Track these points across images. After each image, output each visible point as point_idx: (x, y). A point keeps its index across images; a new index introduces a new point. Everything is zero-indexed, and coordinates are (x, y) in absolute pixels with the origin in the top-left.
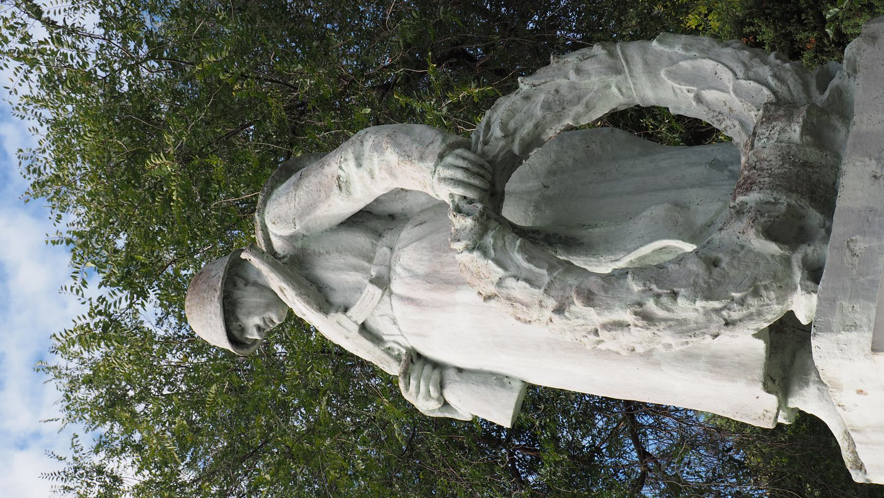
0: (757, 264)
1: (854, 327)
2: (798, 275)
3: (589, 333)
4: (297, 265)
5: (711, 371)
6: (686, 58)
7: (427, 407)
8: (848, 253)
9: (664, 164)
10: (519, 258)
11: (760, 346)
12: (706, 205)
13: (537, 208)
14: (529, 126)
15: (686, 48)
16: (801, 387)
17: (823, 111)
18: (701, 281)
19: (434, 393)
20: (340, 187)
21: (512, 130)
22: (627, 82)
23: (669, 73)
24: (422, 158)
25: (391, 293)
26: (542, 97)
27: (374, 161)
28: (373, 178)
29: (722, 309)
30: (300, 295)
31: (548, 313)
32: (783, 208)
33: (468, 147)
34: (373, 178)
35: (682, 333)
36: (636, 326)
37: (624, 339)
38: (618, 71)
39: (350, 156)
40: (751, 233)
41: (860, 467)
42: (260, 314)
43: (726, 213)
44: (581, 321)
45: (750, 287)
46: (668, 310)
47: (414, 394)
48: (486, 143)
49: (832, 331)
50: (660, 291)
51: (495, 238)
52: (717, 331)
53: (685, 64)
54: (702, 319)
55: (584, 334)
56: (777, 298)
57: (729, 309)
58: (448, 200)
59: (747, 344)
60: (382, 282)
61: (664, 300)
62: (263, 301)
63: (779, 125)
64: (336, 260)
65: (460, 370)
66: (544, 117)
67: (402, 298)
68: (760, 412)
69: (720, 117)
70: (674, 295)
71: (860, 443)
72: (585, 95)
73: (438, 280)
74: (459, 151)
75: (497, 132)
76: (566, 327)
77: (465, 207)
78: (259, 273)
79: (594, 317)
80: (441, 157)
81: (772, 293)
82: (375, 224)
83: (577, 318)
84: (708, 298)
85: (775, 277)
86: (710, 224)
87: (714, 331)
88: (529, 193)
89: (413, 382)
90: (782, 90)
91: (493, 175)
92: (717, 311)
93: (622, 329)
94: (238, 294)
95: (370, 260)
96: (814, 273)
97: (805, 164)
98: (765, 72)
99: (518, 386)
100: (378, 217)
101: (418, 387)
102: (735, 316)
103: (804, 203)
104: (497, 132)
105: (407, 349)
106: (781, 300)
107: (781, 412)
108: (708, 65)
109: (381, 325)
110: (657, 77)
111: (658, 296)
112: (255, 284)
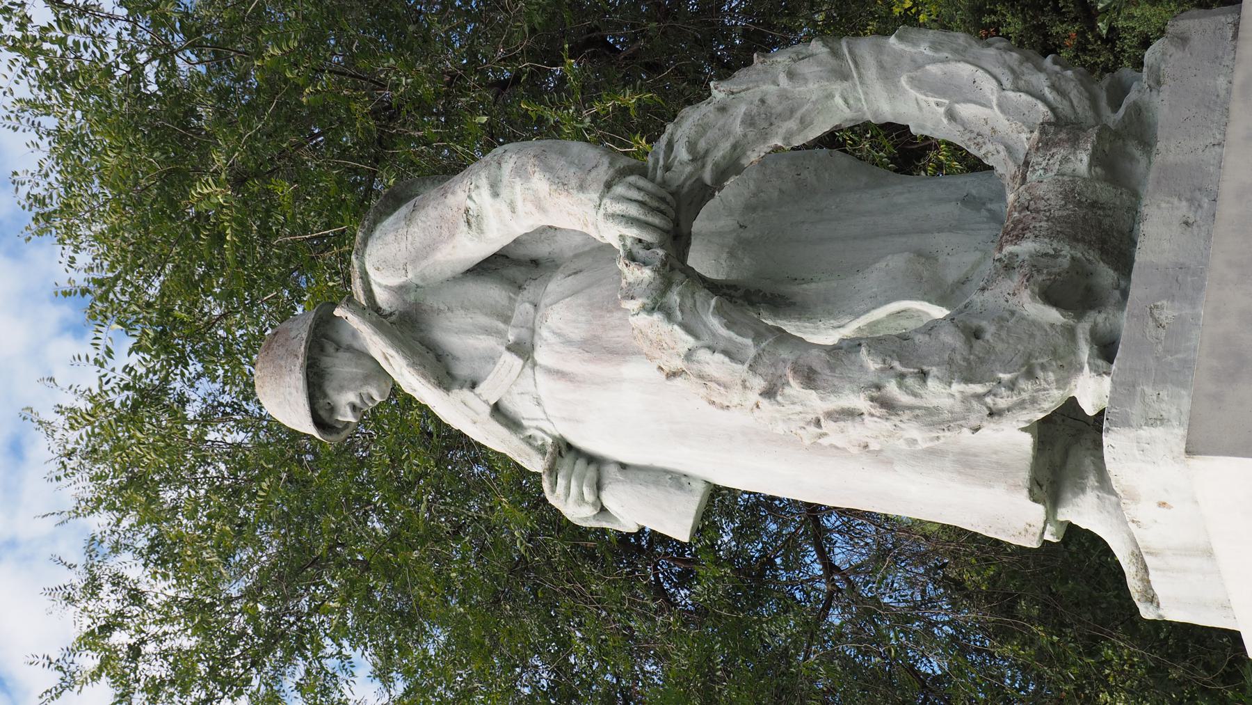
0: (1032, 336)
1: (1160, 421)
2: (1085, 352)
3: (809, 423)
4: (408, 324)
5: (960, 473)
6: (934, 61)
7: (578, 512)
8: (1151, 323)
9: (900, 200)
10: (715, 323)
11: (1027, 440)
12: (960, 255)
13: (732, 254)
14: (723, 148)
15: (935, 46)
16: (1075, 495)
17: (1117, 134)
18: (958, 357)
19: (589, 496)
20: (468, 222)
21: (702, 152)
22: (855, 90)
23: (912, 80)
24: (582, 187)
25: (535, 364)
26: (742, 109)
27: (516, 189)
28: (513, 212)
29: (985, 395)
30: (413, 365)
31: (754, 397)
32: (1065, 262)
33: (643, 172)
34: (513, 212)
35: (932, 425)
36: (872, 415)
37: (854, 432)
38: (845, 77)
39: (484, 182)
40: (1025, 296)
41: (1152, 599)
42: (356, 388)
43: (988, 267)
44: (798, 408)
45: (1023, 366)
46: (915, 395)
47: (562, 498)
48: (667, 168)
49: (1130, 426)
50: (904, 370)
51: (681, 295)
52: (978, 423)
53: (933, 69)
54: (958, 407)
55: (802, 424)
56: (1057, 381)
57: (995, 395)
58: (617, 244)
59: (1013, 439)
60: (523, 349)
61: (910, 381)
62: (359, 371)
63: (1060, 152)
64: (460, 319)
65: (623, 466)
66: (745, 136)
67: (550, 371)
68: (1021, 526)
69: (980, 139)
70: (923, 375)
71: (1156, 569)
72: (800, 106)
73: (595, 347)
74: (632, 179)
75: (682, 153)
76: (777, 415)
77: (641, 253)
78: (354, 334)
79: (816, 403)
80: (608, 186)
81: (1051, 374)
82: (513, 272)
83: (793, 403)
84: (967, 380)
85: (1054, 353)
86: (965, 281)
87: (974, 422)
88: (721, 234)
89: (561, 482)
90: (1063, 106)
91: (677, 210)
92: (979, 397)
93: (853, 420)
94: (326, 361)
95: (506, 320)
96: (1106, 349)
97: (1094, 205)
98: (1040, 81)
99: (700, 489)
100: (518, 262)
101: (568, 488)
102: (1002, 403)
103: (1093, 255)
104: (682, 153)
105: (554, 437)
106: (1062, 383)
107: (1048, 526)
108: (964, 70)
109: (520, 407)
110: (896, 85)
111: (902, 376)
112: (350, 349)
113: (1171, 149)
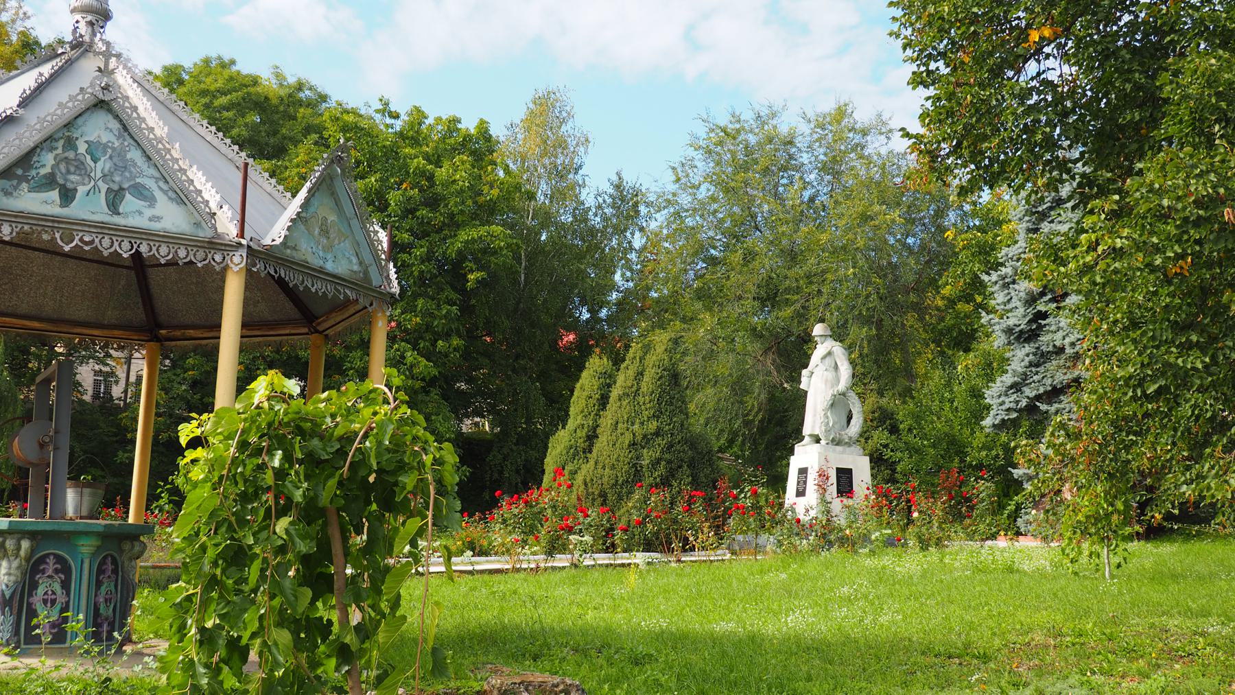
4: (830, 354)
73: (826, 381)
113: (848, 449)
